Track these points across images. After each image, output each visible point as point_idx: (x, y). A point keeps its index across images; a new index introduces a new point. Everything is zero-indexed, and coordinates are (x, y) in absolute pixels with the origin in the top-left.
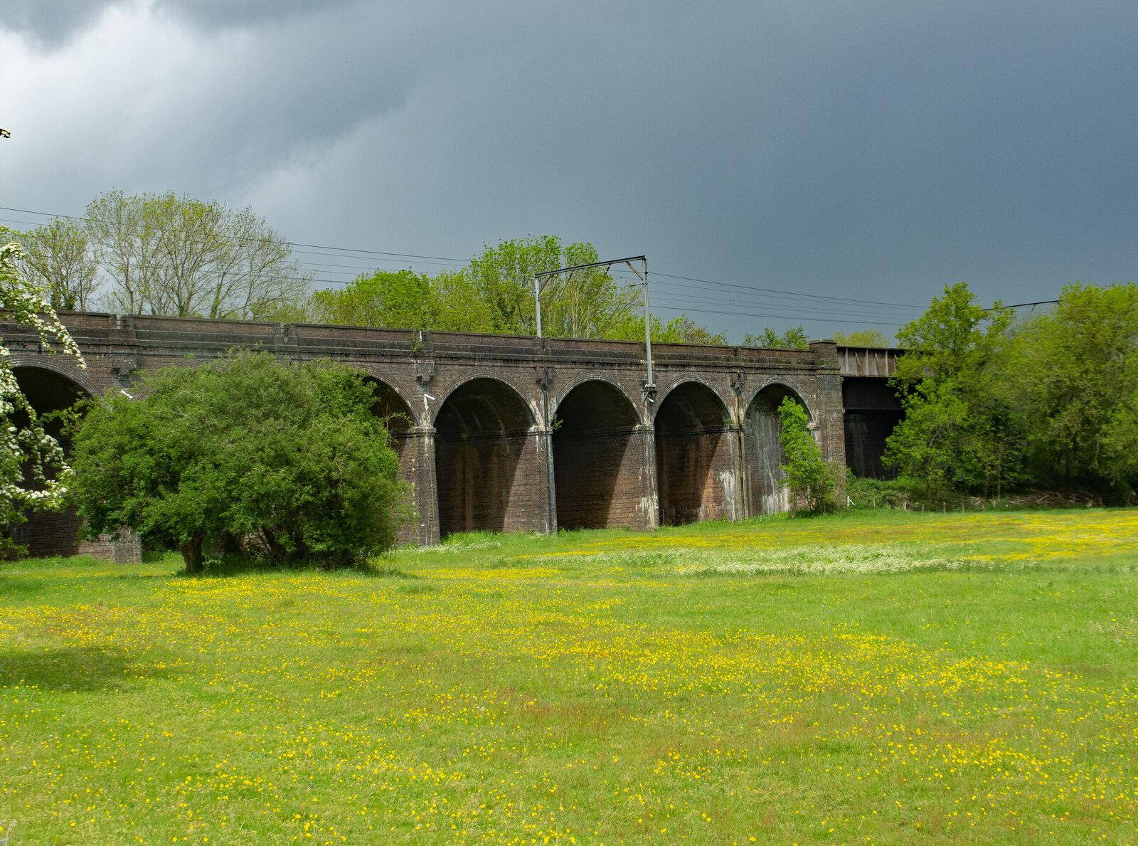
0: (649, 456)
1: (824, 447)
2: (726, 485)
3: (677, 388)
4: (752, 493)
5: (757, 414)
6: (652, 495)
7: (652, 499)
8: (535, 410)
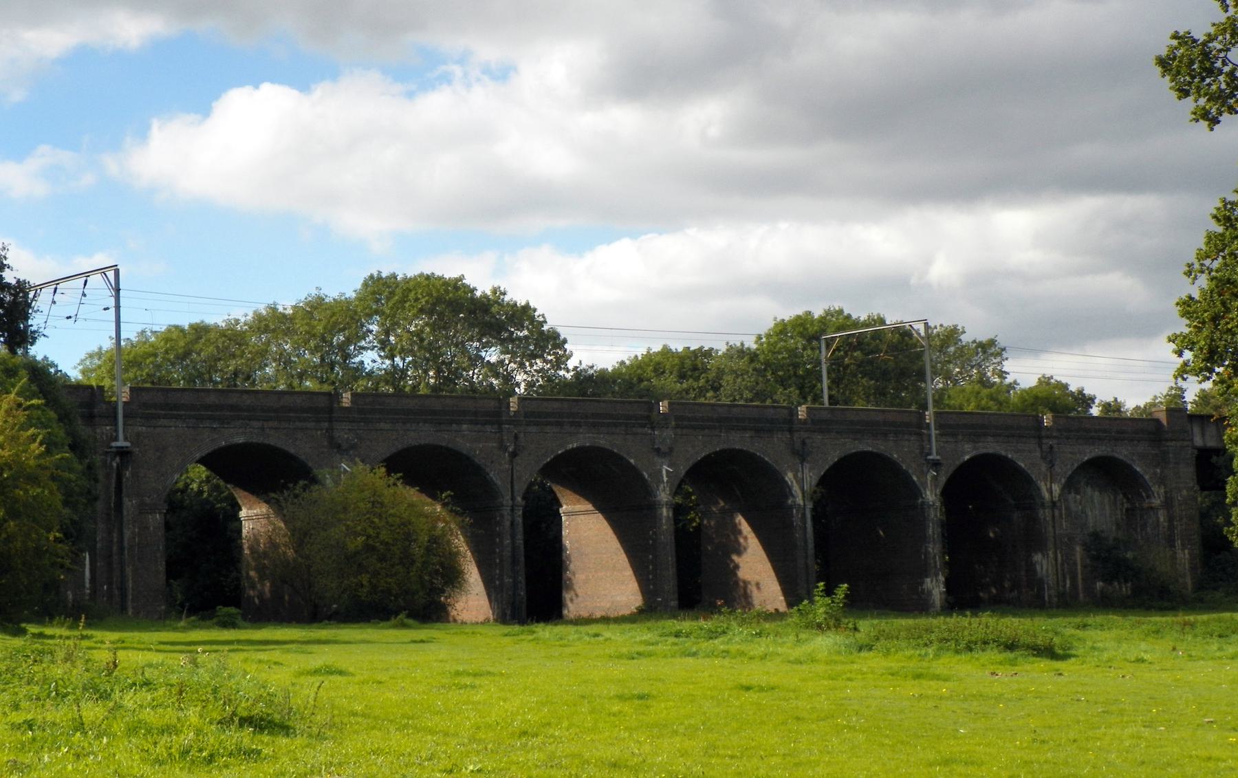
0: (934, 534)
1: (1171, 527)
2: (1038, 568)
3: (968, 460)
4: (1083, 579)
5: (1089, 490)
6: (936, 575)
7: (937, 580)
8: (792, 482)
